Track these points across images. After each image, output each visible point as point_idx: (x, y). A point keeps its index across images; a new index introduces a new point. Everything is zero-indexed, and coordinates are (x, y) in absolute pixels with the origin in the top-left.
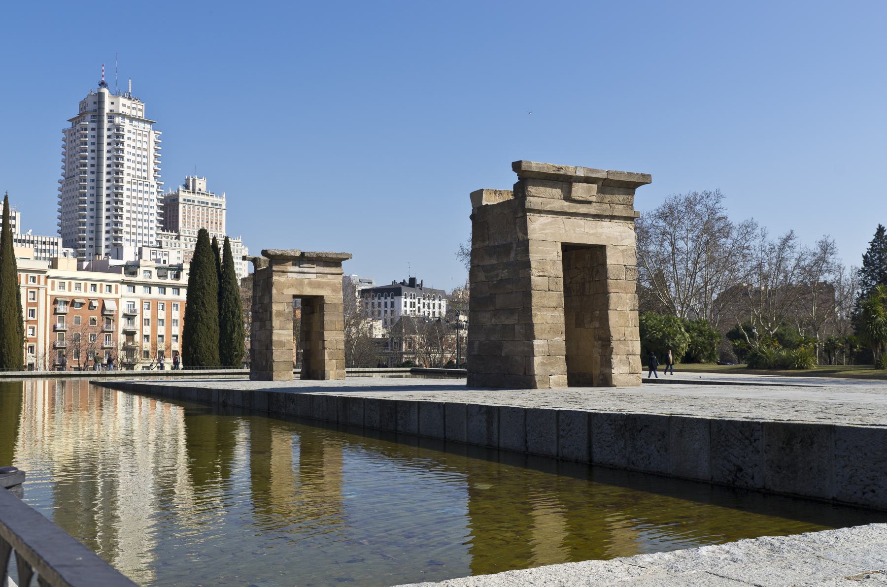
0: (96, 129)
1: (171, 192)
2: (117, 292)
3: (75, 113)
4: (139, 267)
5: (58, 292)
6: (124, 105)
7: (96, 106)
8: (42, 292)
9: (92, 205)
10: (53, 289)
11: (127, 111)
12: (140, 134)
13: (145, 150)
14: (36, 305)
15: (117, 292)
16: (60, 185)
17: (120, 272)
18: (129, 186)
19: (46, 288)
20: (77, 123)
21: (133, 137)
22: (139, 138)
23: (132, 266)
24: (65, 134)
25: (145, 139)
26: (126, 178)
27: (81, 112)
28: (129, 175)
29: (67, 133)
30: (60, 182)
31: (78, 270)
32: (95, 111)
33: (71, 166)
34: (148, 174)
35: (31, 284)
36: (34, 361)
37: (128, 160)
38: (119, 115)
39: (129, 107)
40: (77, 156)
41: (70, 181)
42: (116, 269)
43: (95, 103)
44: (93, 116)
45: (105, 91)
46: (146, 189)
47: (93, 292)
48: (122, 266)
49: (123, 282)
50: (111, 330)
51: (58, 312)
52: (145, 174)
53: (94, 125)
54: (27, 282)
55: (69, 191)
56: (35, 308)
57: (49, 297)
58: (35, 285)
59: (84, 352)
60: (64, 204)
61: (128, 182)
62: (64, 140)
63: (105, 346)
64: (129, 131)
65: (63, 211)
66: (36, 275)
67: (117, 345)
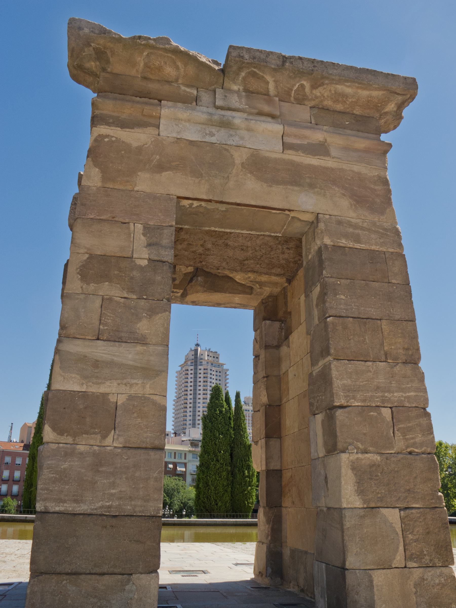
2: (185, 458)
7: (193, 357)
15: (185, 458)
16: (174, 403)
20: (183, 367)
24: (177, 374)
29: (178, 373)
30: (174, 400)
32: (193, 359)
40: (183, 385)
43: (193, 355)
49: (190, 451)
53: (192, 367)
60: (175, 413)
62: (177, 377)
65: (175, 417)
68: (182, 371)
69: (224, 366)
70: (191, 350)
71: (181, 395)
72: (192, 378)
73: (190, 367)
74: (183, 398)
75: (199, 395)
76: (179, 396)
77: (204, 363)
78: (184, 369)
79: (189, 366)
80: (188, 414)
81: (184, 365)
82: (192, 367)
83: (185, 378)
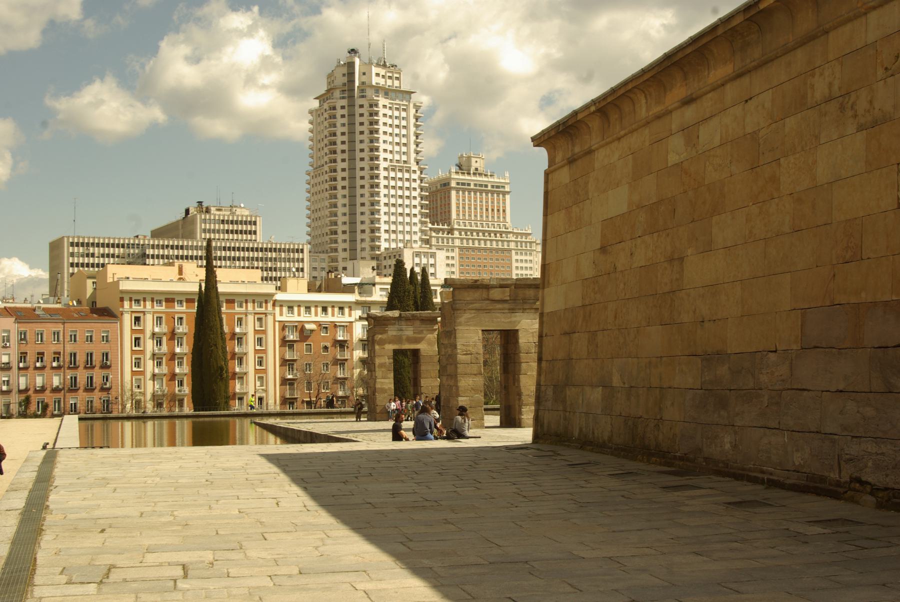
0: (346, 107)
1: (441, 174)
2: (350, 315)
3: (323, 90)
4: (374, 285)
5: (286, 317)
6: (378, 75)
7: (345, 79)
8: (270, 319)
9: (345, 199)
10: (281, 314)
11: (382, 82)
12: (397, 109)
13: (404, 127)
14: (264, 332)
15: (350, 315)
16: (308, 178)
17: (353, 292)
18: (385, 174)
19: (274, 314)
21: (389, 113)
22: (396, 113)
23: (366, 284)
24: (312, 115)
25: (404, 114)
26: (383, 164)
27: (329, 87)
28: (385, 159)
29: (314, 114)
31: (309, 290)
32: (344, 85)
33: (319, 153)
34: (409, 157)
35: (258, 310)
36: (264, 395)
37: (385, 142)
38: (372, 86)
39: (383, 77)
41: (319, 172)
42: (349, 289)
43: (344, 75)
44: (343, 91)
45: (357, 61)
46: (407, 175)
47: (324, 315)
48: (356, 284)
50: (346, 358)
51: (287, 339)
52: (404, 158)
53: (344, 102)
54: (254, 308)
55: (318, 185)
56: (263, 336)
57: (277, 324)
58: (263, 310)
59: (315, 383)
61: (385, 169)
63: (339, 376)
64: (385, 106)
66: (263, 299)
67: (352, 375)
68: (323, 111)
69: (412, 95)
70: (339, 65)
71: (323, 162)
72: (344, 125)
73: (339, 100)
74: (326, 168)
75: (362, 162)
76: (319, 164)
77: (369, 93)
78: (326, 106)
79: (337, 99)
80: (341, 201)
81: (325, 97)
82: (344, 102)
83: (330, 126)
